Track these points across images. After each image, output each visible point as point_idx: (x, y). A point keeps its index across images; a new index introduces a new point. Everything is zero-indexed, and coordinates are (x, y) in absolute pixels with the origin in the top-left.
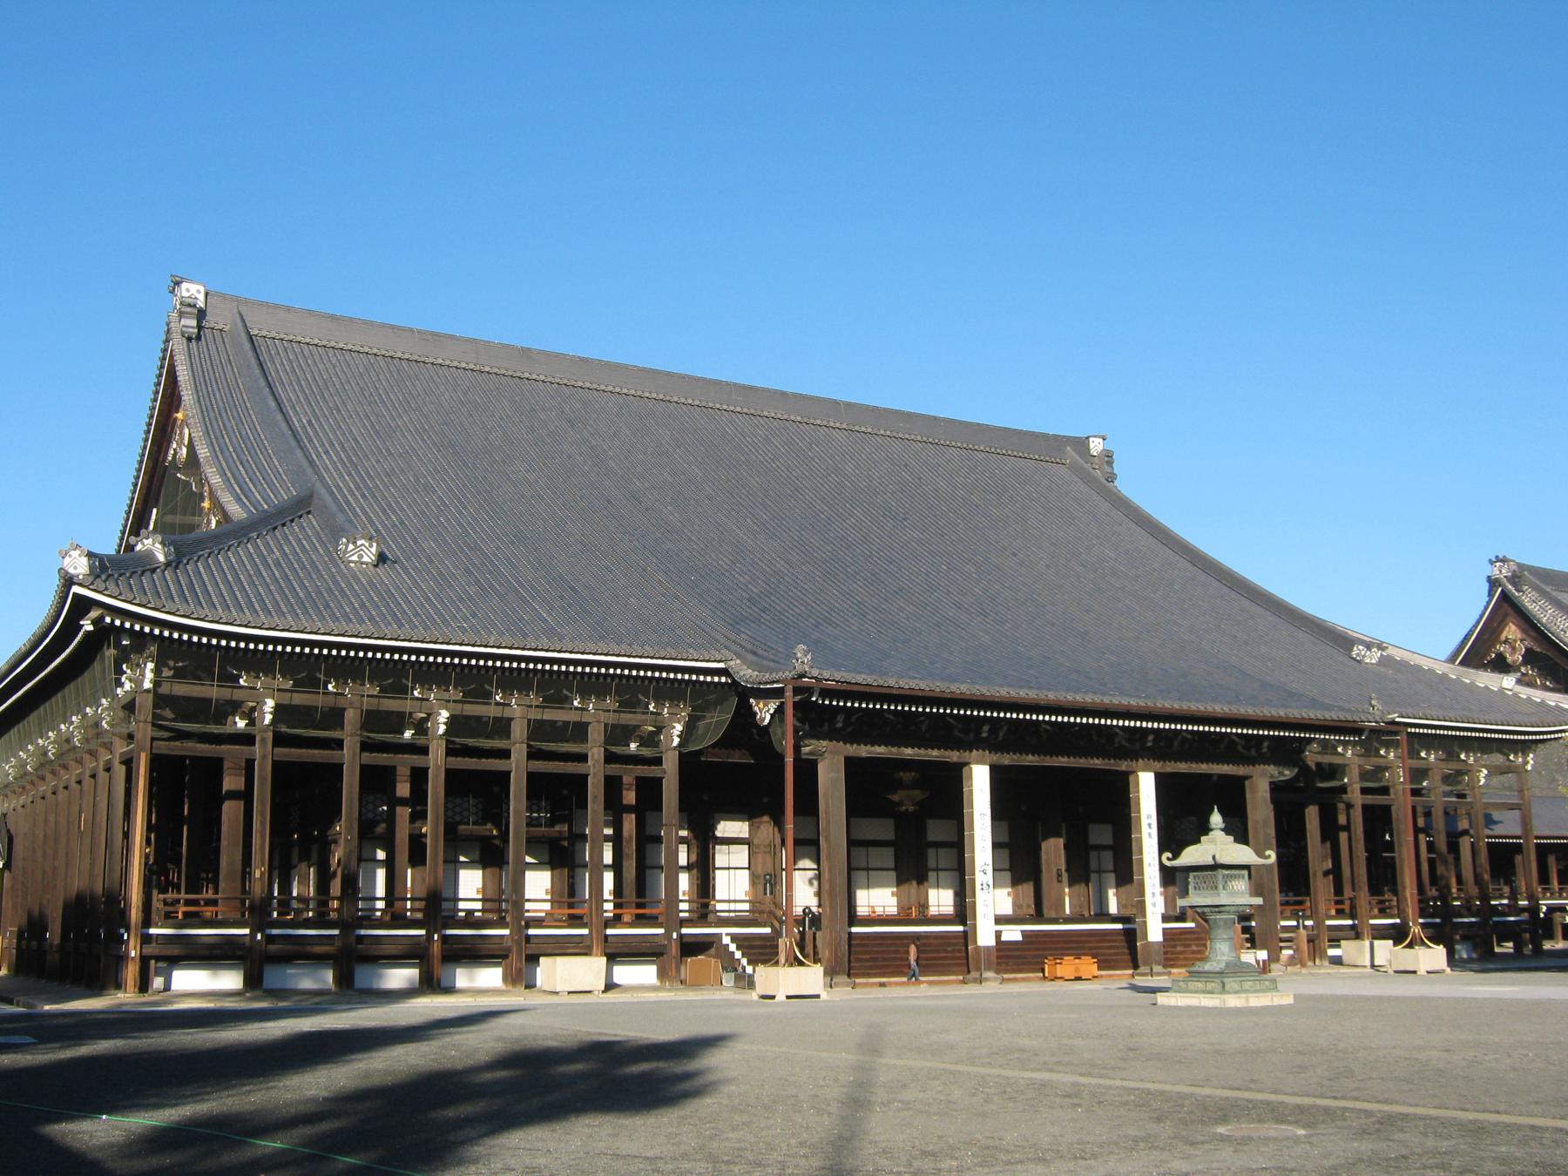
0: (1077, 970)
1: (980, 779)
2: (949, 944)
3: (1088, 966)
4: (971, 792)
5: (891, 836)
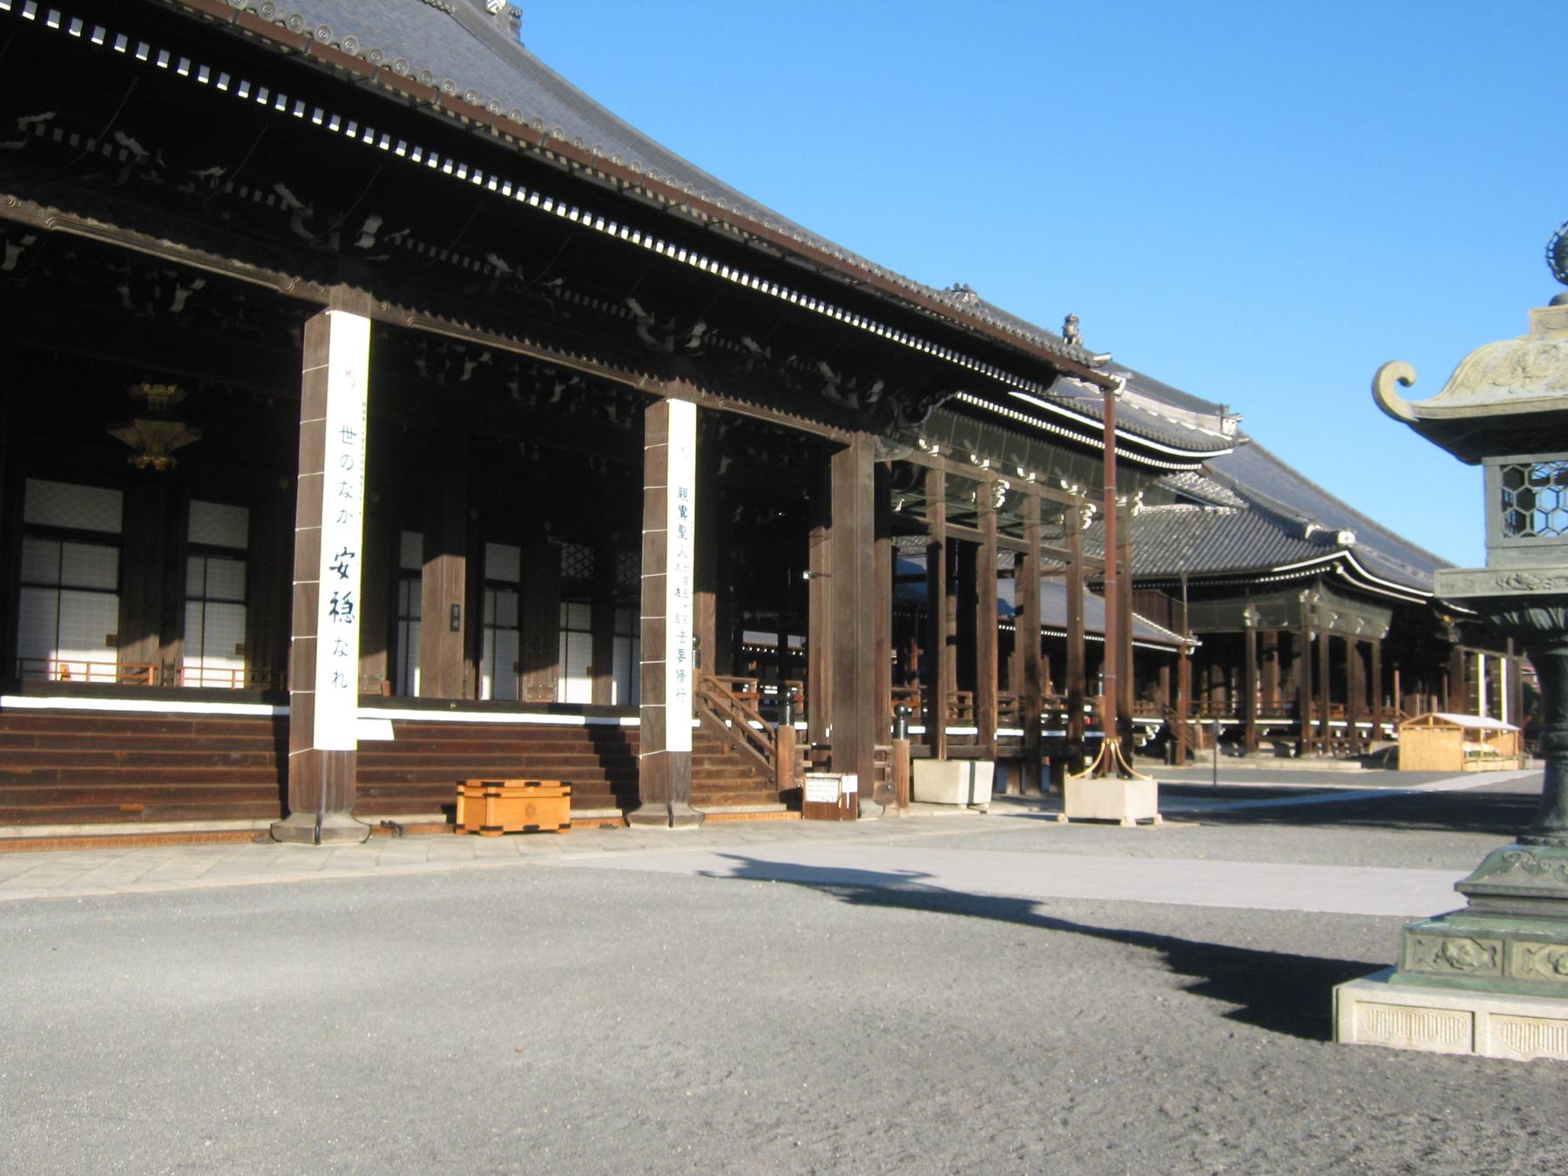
0: (530, 810)
1: (346, 345)
2: (236, 745)
3: (552, 802)
4: (322, 376)
5: (114, 525)
